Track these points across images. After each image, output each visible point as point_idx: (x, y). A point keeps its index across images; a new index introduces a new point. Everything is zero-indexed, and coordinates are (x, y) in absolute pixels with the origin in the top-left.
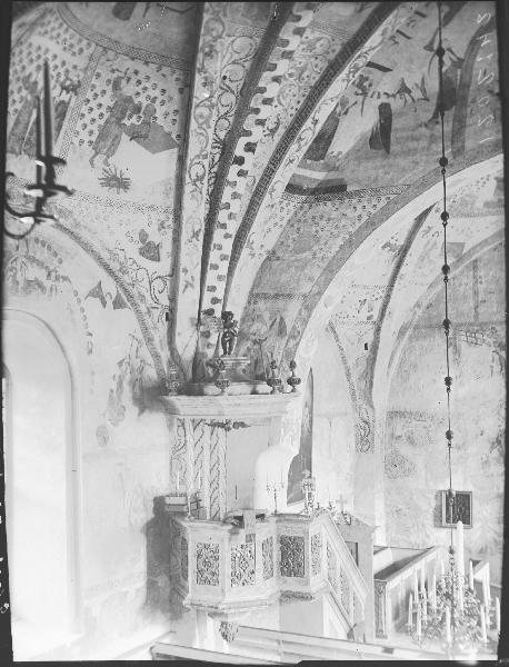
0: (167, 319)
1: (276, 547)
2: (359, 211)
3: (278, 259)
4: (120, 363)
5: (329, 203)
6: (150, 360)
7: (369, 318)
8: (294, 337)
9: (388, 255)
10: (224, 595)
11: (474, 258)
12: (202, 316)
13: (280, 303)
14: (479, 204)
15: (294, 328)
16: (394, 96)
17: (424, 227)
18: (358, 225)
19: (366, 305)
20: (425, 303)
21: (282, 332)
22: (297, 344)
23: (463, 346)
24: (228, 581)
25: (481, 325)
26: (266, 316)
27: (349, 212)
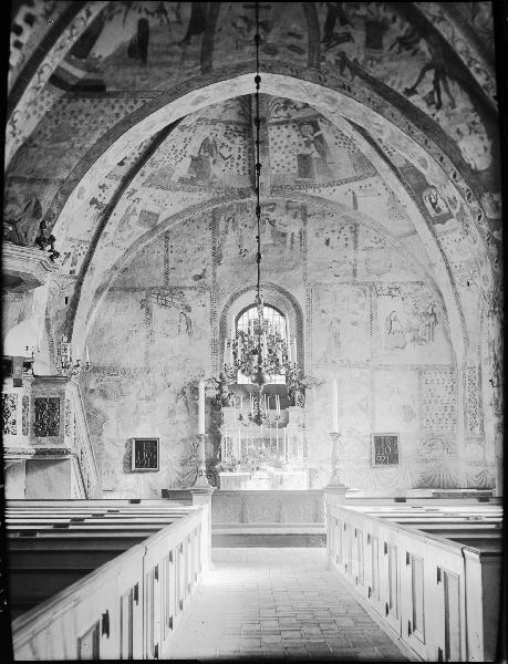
2: (116, 110)
3: (35, 146)
5: (88, 101)
8: (50, 220)
9: (94, 211)
11: (166, 229)
13: (36, 188)
14: (175, 178)
16: (153, 14)
17: (128, 189)
18: (116, 122)
19: (70, 259)
20: (122, 266)
21: (37, 213)
23: (155, 308)
25: (171, 289)
26: (21, 199)
27: (108, 110)
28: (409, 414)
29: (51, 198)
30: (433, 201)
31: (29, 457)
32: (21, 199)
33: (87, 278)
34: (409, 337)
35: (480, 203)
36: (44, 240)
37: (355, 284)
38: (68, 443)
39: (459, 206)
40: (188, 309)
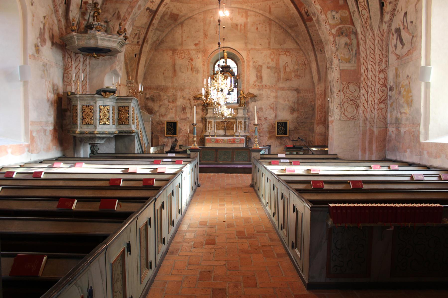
0: (65, 3)
1: (116, 111)
4: (45, 17)
6: (56, 22)
7: (138, 42)
8: (124, 20)
10: (96, 128)
12: (82, 5)
13: (118, 5)
15: (124, 16)
21: (119, 17)
22: (126, 23)
24: (98, 122)
26: (111, 10)
28: (293, 110)
29: (125, 10)
30: (306, 11)
31: (115, 135)
32: (111, 10)
33: (145, 44)
34: (293, 75)
35: (326, 17)
36: (121, 32)
37: (269, 48)
38: (133, 128)
39: (316, 17)
40: (192, 60)
